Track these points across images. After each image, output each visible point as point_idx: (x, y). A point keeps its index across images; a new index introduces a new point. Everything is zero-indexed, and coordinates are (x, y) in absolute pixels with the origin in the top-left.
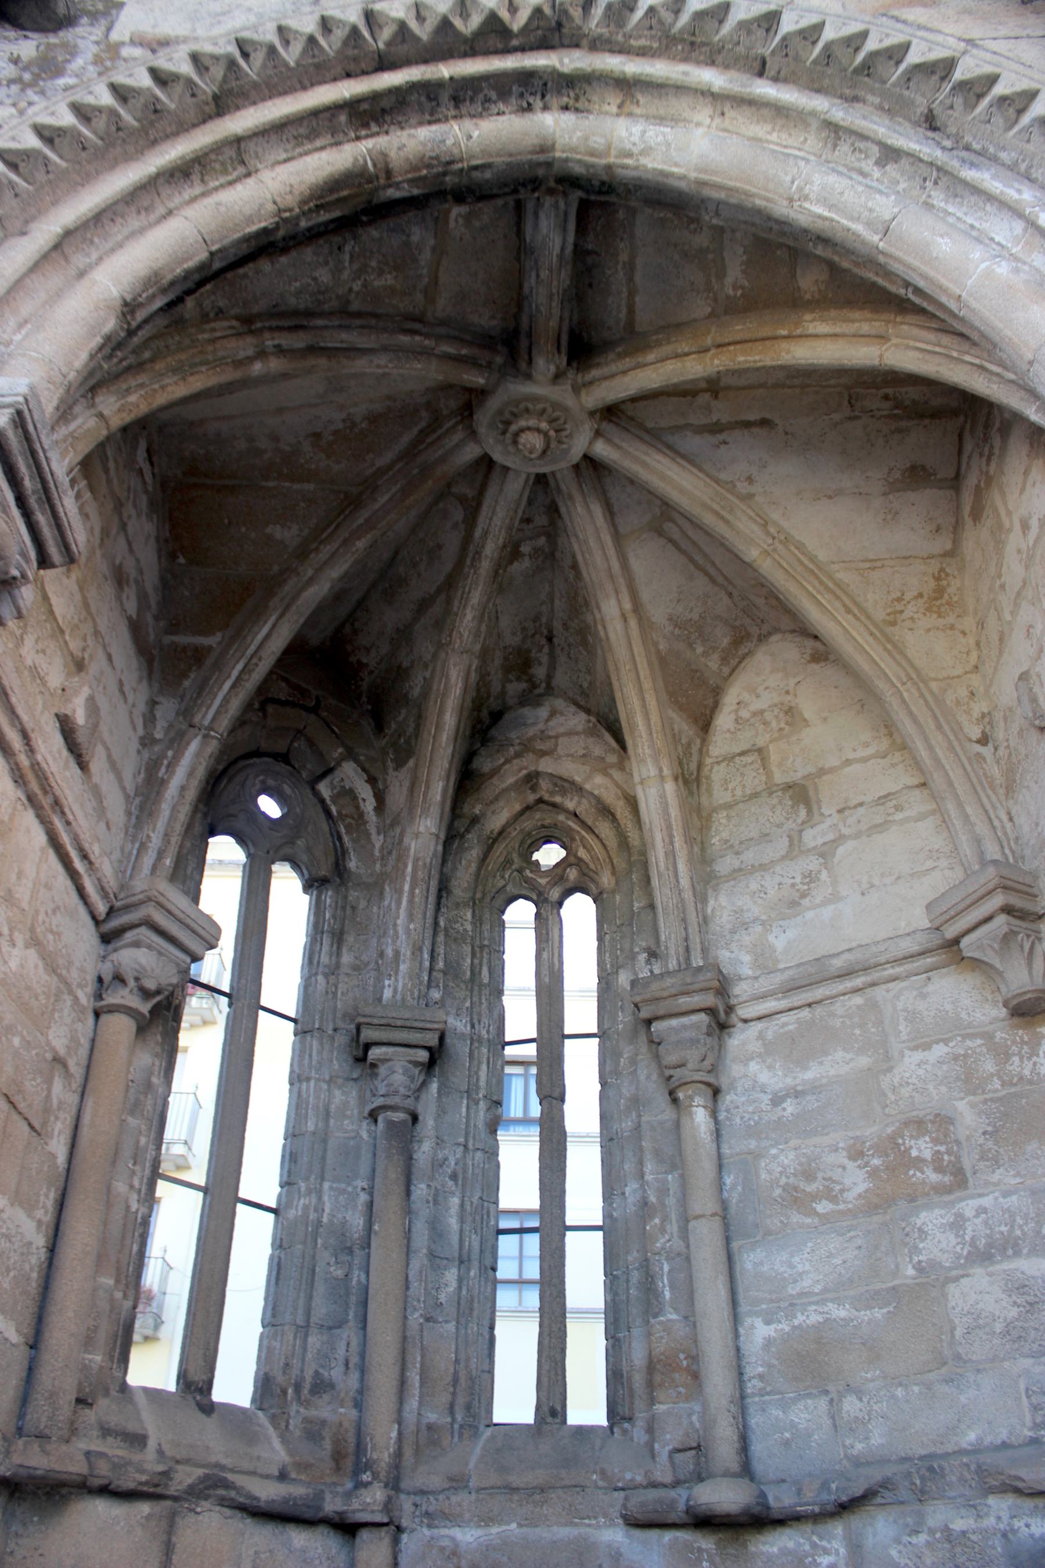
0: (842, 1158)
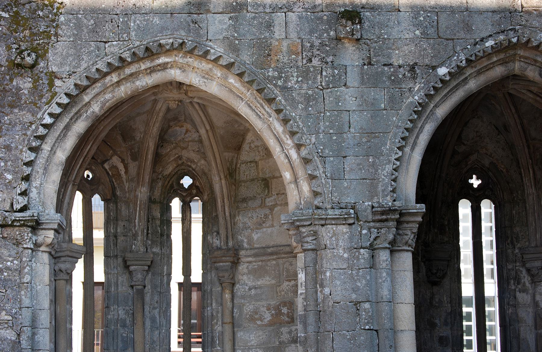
0: (264, 309)
